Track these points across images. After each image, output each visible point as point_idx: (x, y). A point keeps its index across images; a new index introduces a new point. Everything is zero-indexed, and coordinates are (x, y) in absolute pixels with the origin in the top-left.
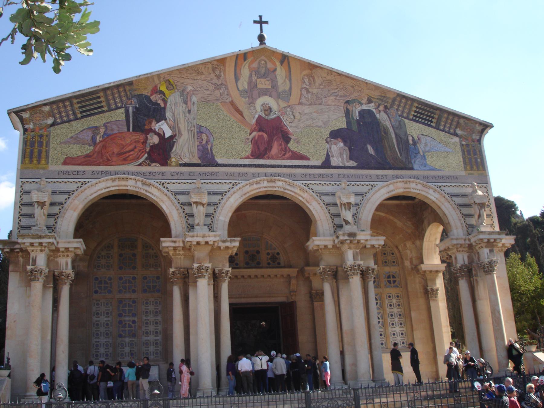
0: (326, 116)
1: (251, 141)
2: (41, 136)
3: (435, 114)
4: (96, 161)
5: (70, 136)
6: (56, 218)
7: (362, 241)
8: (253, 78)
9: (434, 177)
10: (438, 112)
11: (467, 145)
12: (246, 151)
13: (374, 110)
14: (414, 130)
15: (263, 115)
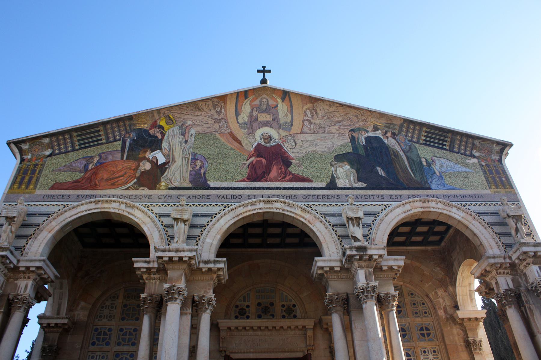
0: (331, 143)
1: (248, 166)
2: (36, 165)
3: (447, 138)
4: (84, 186)
6: (29, 239)
7: (375, 257)
8: (254, 113)
10: (450, 135)
11: (487, 165)
12: (241, 175)
13: (381, 137)
15: (263, 143)
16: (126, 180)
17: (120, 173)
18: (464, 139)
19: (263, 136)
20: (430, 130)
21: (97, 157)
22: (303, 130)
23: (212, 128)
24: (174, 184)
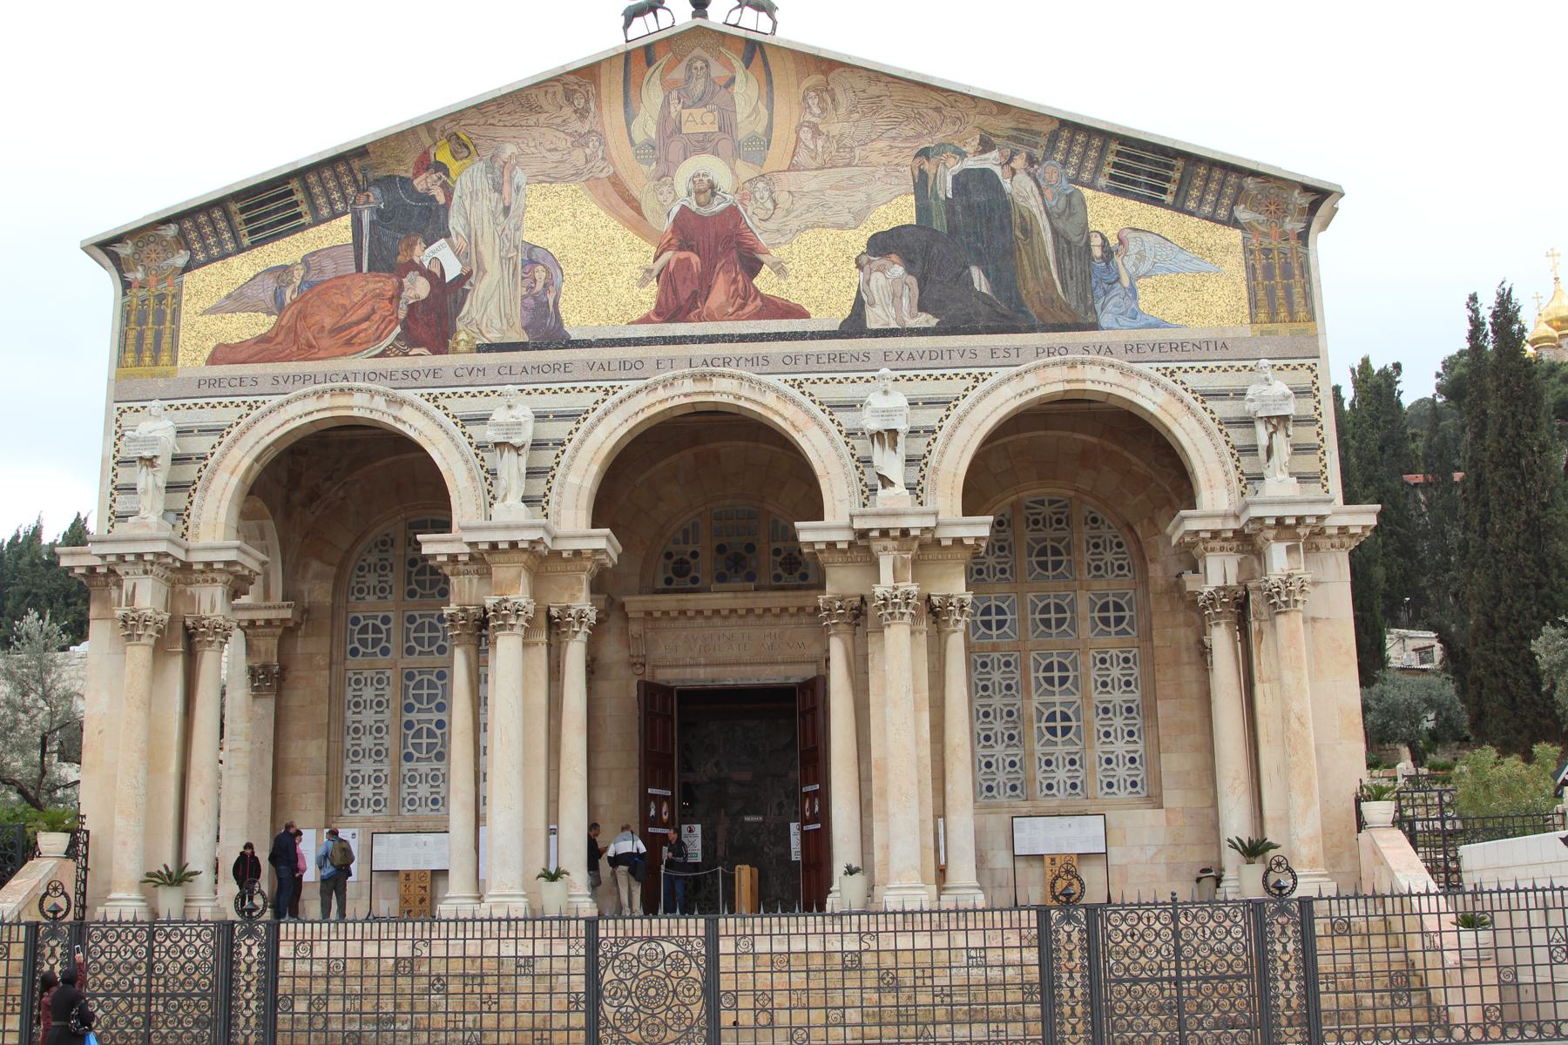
0: (863, 196)
1: (658, 276)
2: (161, 298)
7: (913, 533)
8: (672, 109)
9: (1157, 346)
10: (1179, 163)
13: (998, 170)
15: (694, 207)
18: (1217, 174)
21: (300, 267)
24: (488, 336)
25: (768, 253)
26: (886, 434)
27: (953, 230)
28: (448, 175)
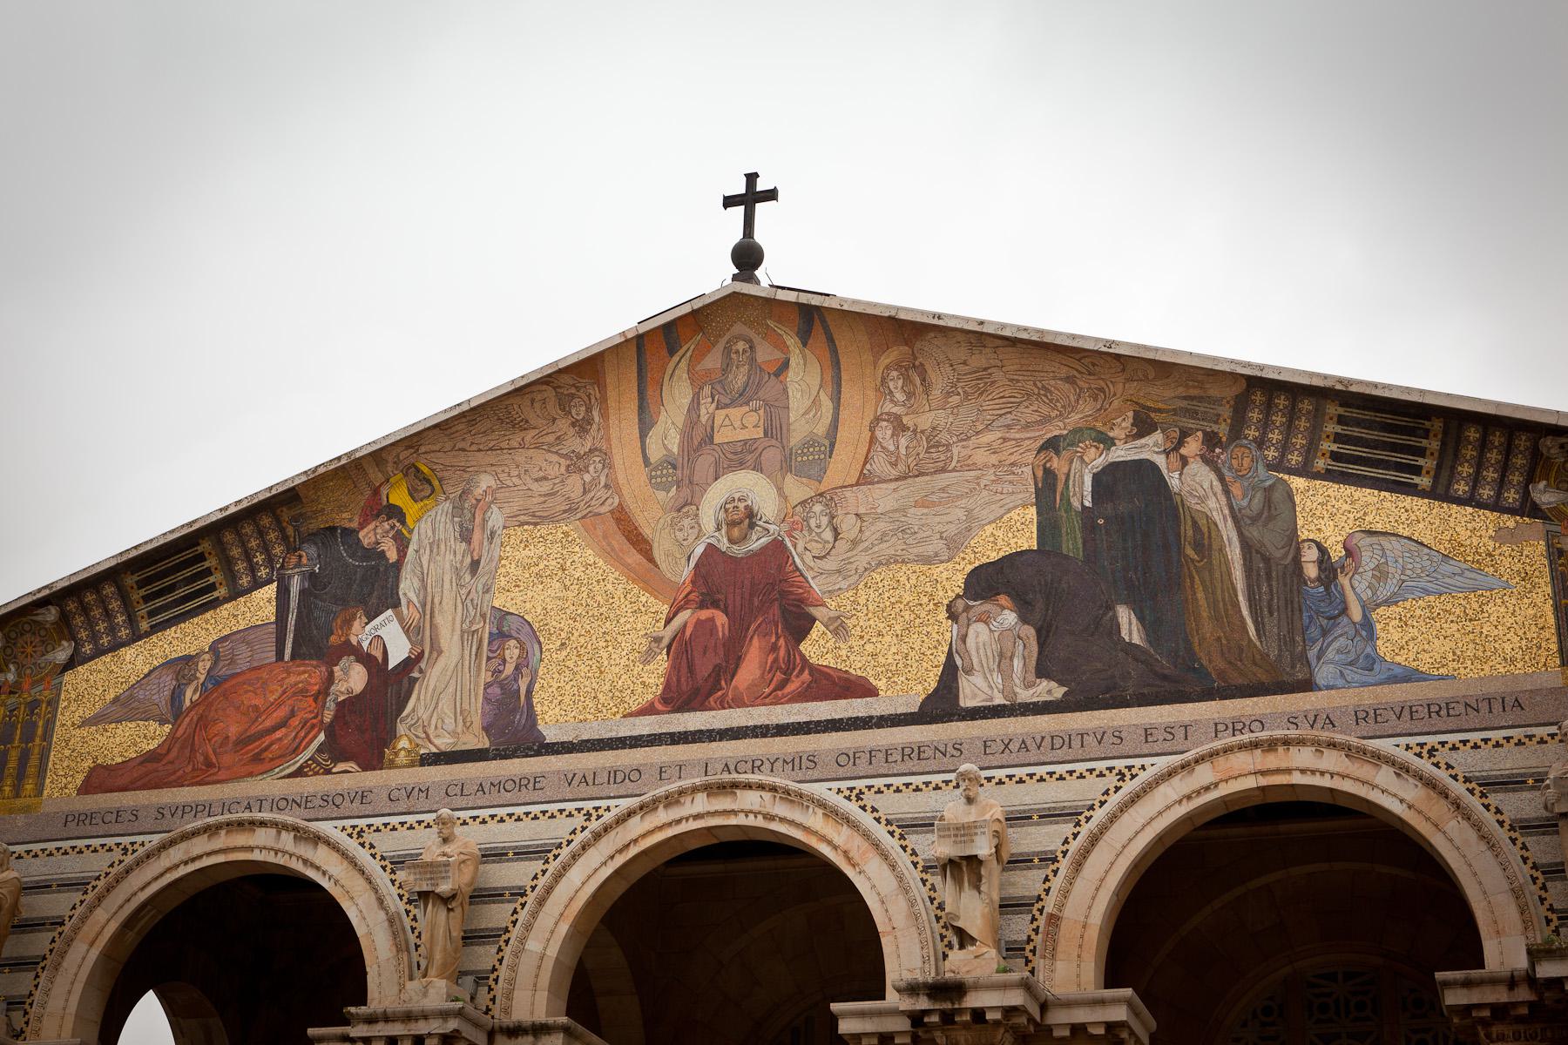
0: (961, 514)
1: (669, 647)
4: (175, 773)
5: (112, 696)
6: (39, 970)
8: (703, 411)
9: (1406, 711)
13: (1160, 461)
14: (1332, 515)
15: (724, 545)
16: (296, 737)
17: (275, 715)
19: (726, 511)
20: (1355, 413)
21: (207, 657)
22: (868, 466)
23: (559, 499)
24: (436, 741)
25: (823, 605)
26: (964, 863)
27: (1091, 556)
28: (403, 522)
